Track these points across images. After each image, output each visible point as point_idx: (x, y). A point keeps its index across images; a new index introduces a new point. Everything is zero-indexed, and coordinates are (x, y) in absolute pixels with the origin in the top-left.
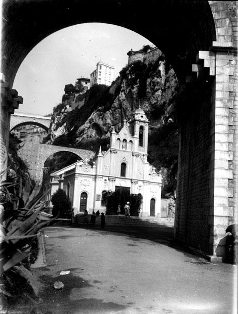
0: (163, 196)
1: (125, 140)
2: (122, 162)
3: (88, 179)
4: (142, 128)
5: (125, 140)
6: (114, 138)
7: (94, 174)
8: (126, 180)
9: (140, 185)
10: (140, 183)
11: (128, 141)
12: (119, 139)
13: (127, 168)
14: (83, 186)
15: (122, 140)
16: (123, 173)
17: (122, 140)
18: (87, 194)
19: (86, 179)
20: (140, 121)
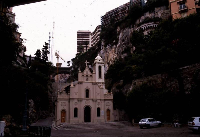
0: (115, 108)
1: (87, 76)
2: (86, 89)
4: (100, 68)
5: (87, 76)
6: (80, 75)
7: (69, 98)
9: (98, 102)
10: (99, 101)
11: (89, 76)
12: (83, 75)
14: (62, 106)
17: (85, 75)
18: (65, 111)
20: (98, 63)
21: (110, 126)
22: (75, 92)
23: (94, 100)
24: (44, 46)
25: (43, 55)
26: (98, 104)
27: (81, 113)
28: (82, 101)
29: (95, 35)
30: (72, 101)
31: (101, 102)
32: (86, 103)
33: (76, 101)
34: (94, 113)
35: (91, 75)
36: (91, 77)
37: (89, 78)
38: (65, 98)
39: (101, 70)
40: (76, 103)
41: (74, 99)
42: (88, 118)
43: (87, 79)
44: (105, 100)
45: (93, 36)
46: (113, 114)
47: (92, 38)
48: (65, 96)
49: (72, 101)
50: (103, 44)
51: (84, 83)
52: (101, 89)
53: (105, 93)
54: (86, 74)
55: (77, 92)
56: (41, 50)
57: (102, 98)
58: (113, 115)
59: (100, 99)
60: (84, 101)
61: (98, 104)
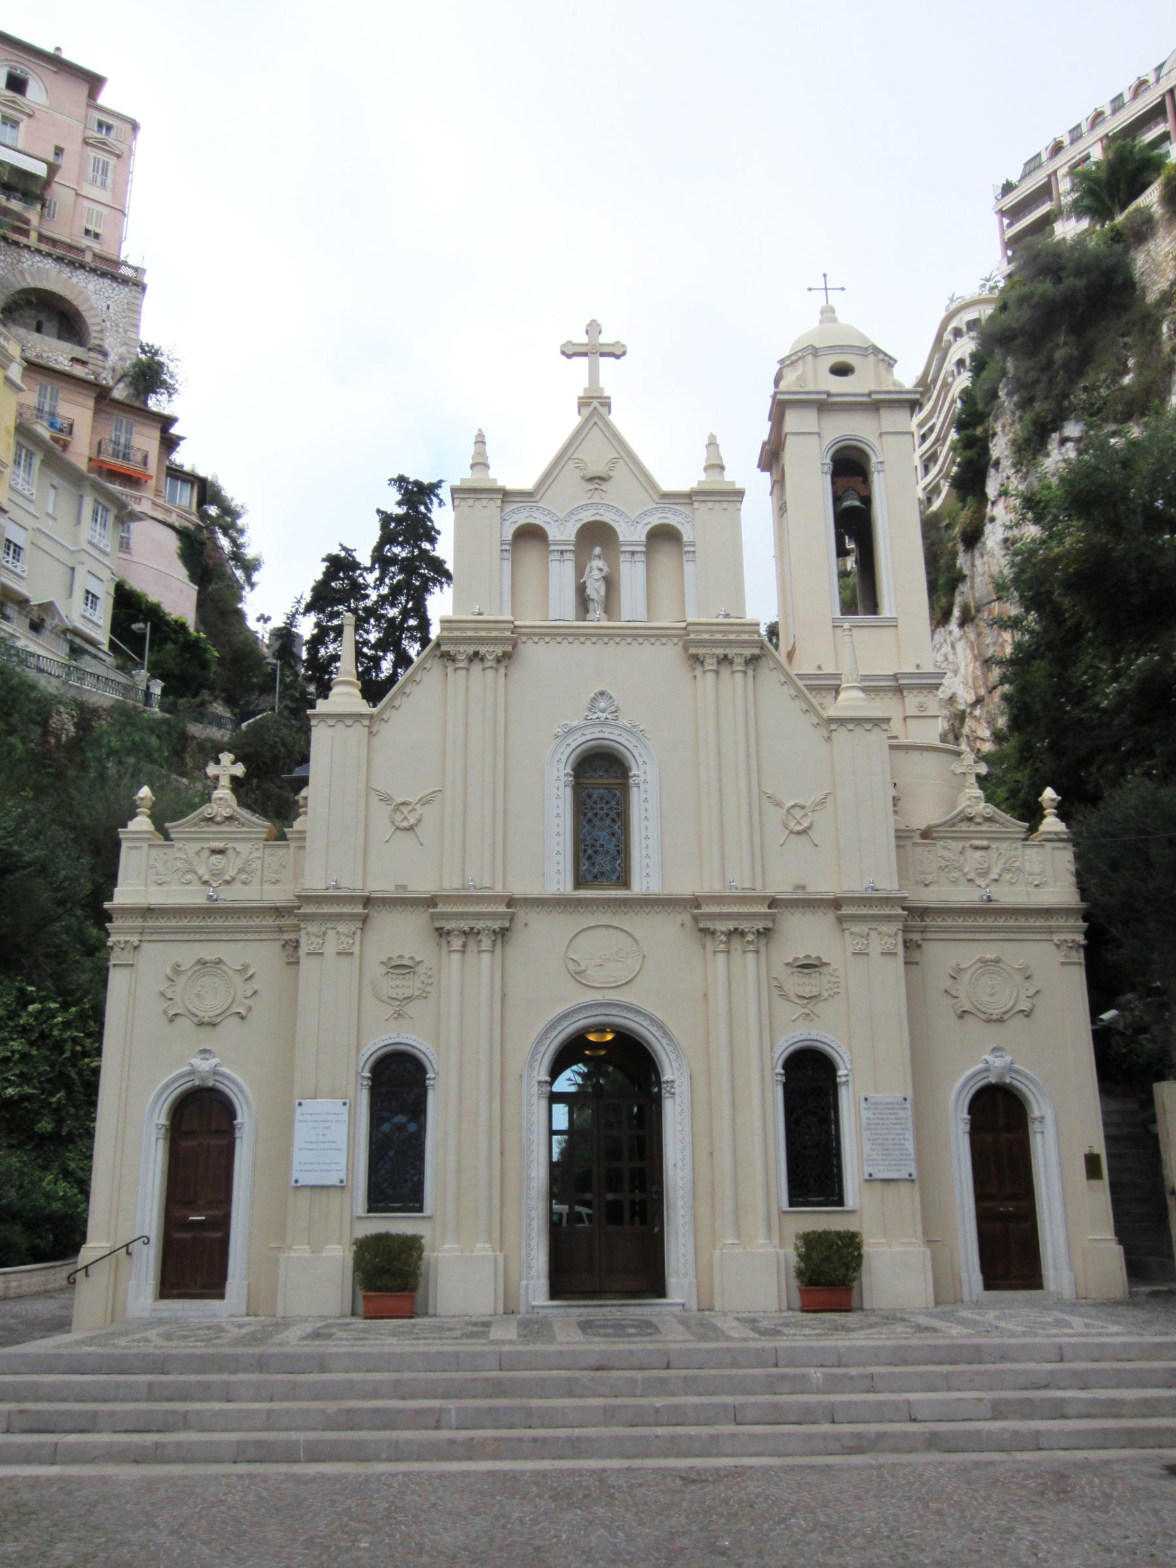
1: (596, 535)
3: (232, 954)
5: (596, 535)
8: (641, 925)
9: (801, 950)
10: (805, 935)
11: (631, 533)
13: (635, 796)
14: (185, 1024)
17: (562, 533)
19: (209, 952)
21: (999, 1410)
22: (385, 799)
23: (738, 924)
24: (386, 519)
25: (388, 600)
26: (779, 970)
28: (503, 934)
31: (851, 944)
32: (578, 976)
33: (399, 934)
35: (656, 520)
36: (665, 557)
37: (632, 576)
38: (230, 895)
39: (867, 500)
40: (401, 968)
41: (368, 901)
43: (596, 590)
44: (916, 923)
48: (230, 865)
49: (330, 949)
50: (1000, 448)
51: (531, 651)
52: (841, 735)
53: (926, 811)
54: (587, 517)
55: (425, 801)
56: (364, 557)
57: (875, 871)
59: (836, 903)
60: (542, 935)
61: (797, 984)
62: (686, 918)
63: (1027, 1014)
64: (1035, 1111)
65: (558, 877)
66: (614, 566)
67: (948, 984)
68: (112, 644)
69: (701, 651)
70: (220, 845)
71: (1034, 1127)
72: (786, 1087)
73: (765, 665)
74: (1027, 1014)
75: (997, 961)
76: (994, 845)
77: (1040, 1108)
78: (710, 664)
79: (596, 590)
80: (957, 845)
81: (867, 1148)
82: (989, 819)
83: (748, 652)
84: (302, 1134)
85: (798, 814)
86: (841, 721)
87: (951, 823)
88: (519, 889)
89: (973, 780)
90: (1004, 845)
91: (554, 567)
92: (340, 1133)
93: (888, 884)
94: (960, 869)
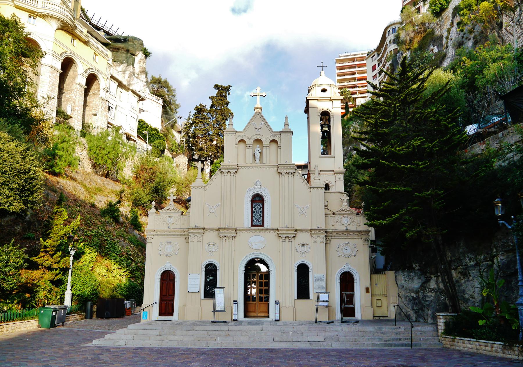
9: (302, 242)
10: (302, 237)
11: (266, 142)
15: (250, 142)
16: (257, 220)
17: (250, 142)
19: (169, 240)
27: (232, 285)
29: (383, 56)
30: (196, 239)
34: (282, 284)
37: (265, 151)
42: (257, 301)
43: (258, 155)
44: (328, 234)
45: (375, 62)
46: (367, 290)
47: (374, 68)
49: (196, 240)
51: (241, 170)
52: (313, 190)
58: (369, 295)
59: (311, 231)
62: (276, 233)
63: (355, 256)
64: (355, 278)
65: (247, 223)
66: (262, 150)
67: (337, 249)
68: (138, 136)
69: (281, 171)
70: (171, 216)
71: (355, 281)
72: (297, 272)
73: (295, 174)
74: (355, 256)
75: (349, 243)
76: (349, 216)
77: (356, 277)
78: (283, 174)
79: (258, 155)
80: (339, 216)
81: (315, 286)
82: (349, 210)
83: (292, 171)
84: (190, 281)
85: (302, 210)
86: (314, 188)
87: (339, 211)
88: (238, 226)
89: (345, 200)
90: (351, 216)
91: (248, 150)
92: (198, 281)
93: (322, 226)
94: (341, 222)
